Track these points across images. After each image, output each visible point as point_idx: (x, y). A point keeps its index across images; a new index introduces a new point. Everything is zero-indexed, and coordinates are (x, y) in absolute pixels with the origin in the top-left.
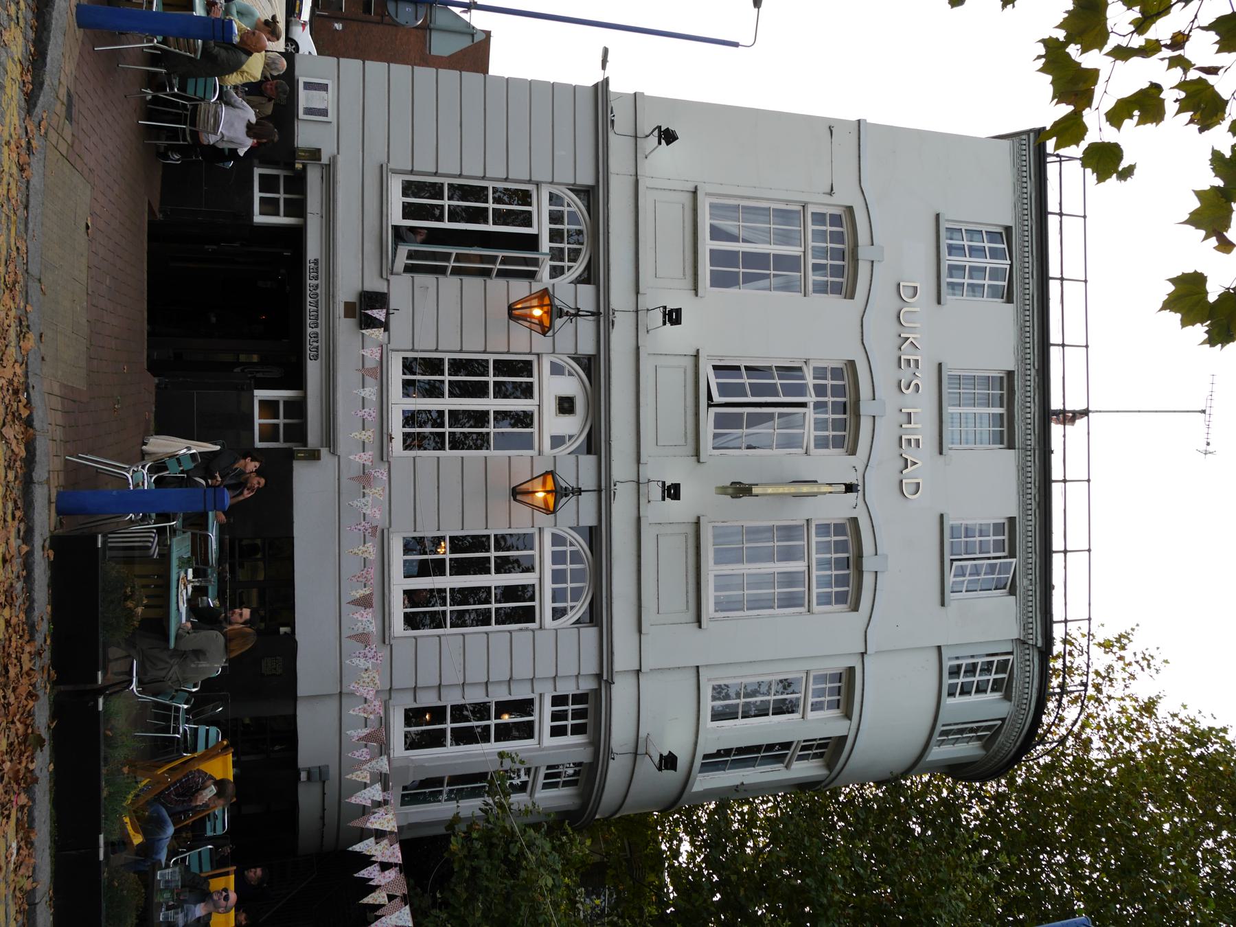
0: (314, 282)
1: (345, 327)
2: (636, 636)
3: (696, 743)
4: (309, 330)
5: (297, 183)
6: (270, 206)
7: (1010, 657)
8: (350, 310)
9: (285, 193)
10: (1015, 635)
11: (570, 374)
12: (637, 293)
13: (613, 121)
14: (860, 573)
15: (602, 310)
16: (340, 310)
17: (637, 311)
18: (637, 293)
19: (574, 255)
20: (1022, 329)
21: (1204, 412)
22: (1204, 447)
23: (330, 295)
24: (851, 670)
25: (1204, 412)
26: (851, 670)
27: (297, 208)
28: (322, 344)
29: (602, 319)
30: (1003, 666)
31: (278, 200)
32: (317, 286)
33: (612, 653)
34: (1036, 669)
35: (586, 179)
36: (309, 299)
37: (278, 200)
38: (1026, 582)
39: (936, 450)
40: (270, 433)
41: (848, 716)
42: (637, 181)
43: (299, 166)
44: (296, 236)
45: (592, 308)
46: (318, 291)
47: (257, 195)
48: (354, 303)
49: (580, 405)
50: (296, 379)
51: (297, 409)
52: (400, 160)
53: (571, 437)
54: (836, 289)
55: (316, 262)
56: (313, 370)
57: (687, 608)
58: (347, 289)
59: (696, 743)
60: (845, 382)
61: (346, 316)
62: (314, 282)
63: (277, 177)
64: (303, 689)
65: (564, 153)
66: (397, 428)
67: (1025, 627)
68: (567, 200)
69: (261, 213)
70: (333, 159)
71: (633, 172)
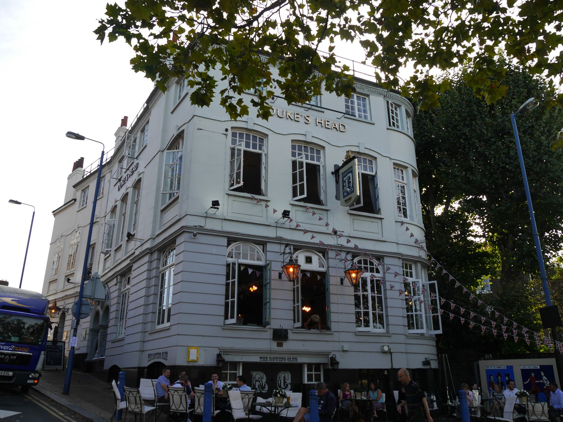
0: (268, 359)
1: (288, 346)
2: (386, 243)
3: (416, 225)
4: (286, 361)
8: (280, 345)
9: (227, 370)
11: (297, 257)
12: (269, 226)
13: (200, 226)
14: (364, 154)
15: (286, 243)
16: (280, 348)
17: (277, 227)
18: (269, 226)
19: (372, 264)
23: (276, 352)
24: (394, 164)
26: (394, 164)
27: (234, 365)
29: (290, 243)
31: (230, 373)
32: (270, 358)
33: (394, 253)
34: (394, 94)
35: (225, 241)
36: (275, 361)
37: (230, 373)
39: (322, 113)
40: (318, 378)
41: (406, 168)
42: (225, 219)
45: (283, 246)
46: (272, 357)
48: (277, 343)
49: (309, 254)
51: (310, 366)
53: (319, 259)
54: (261, 140)
55: (261, 358)
56: (301, 360)
57: (377, 222)
58: (274, 345)
59: (416, 225)
60: (297, 145)
62: (268, 359)
65: (214, 250)
67: (380, 94)
68: (230, 250)
71: (220, 221)
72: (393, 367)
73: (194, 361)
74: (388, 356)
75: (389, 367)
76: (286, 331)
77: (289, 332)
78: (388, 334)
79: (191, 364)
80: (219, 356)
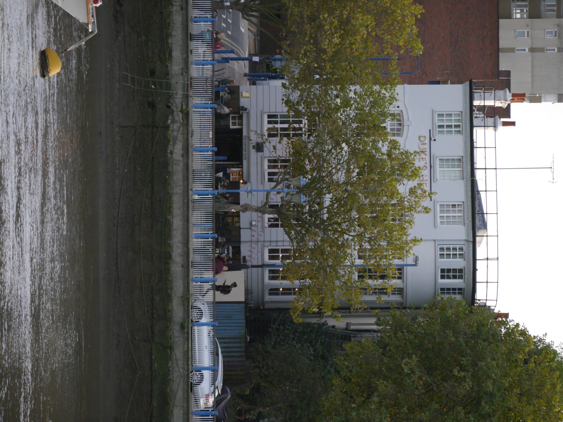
1: (253, 152)
4: (244, 153)
5: (241, 118)
6: (234, 124)
7: (464, 246)
10: (464, 238)
20: (465, 143)
21: (551, 168)
22: (552, 180)
25: (551, 168)
27: (241, 124)
28: (247, 156)
30: (461, 249)
38: (467, 222)
43: (241, 113)
44: (240, 131)
47: (231, 121)
50: (240, 165)
51: (241, 175)
52: (266, 110)
55: (245, 136)
56: (245, 162)
58: (254, 142)
61: (253, 149)
63: (236, 117)
64: (242, 240)
66: (267, 177)
67: (468, 236)
69: (232, 126)
70: (249, 110)
72: (241, 230)
73: (242, 95)
74: (248, 226)
75: (241, 227)
76: (262, 151)
77: (262, 153)
78: (263, 227)
79: (240, 94)
80: (246, 109)
